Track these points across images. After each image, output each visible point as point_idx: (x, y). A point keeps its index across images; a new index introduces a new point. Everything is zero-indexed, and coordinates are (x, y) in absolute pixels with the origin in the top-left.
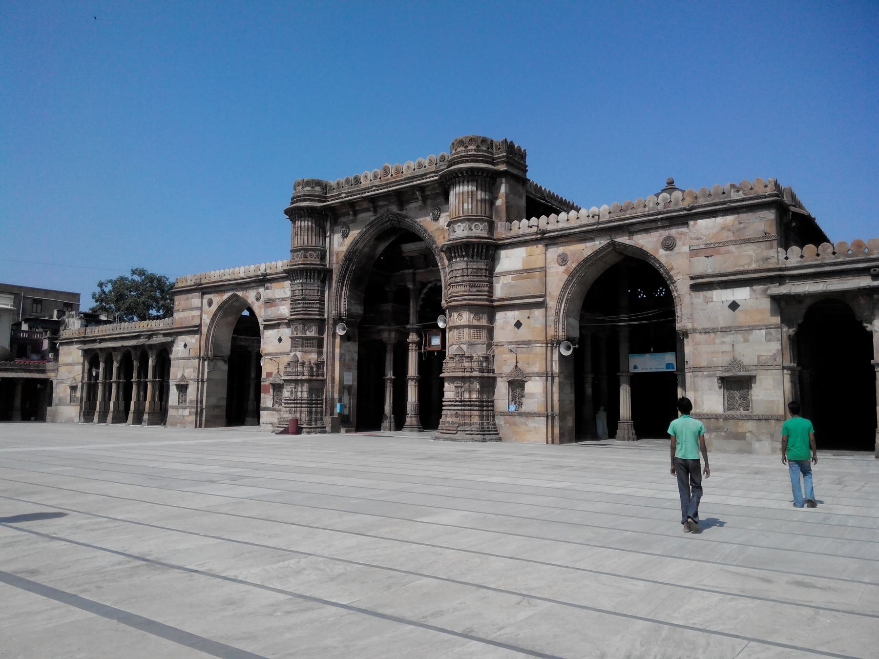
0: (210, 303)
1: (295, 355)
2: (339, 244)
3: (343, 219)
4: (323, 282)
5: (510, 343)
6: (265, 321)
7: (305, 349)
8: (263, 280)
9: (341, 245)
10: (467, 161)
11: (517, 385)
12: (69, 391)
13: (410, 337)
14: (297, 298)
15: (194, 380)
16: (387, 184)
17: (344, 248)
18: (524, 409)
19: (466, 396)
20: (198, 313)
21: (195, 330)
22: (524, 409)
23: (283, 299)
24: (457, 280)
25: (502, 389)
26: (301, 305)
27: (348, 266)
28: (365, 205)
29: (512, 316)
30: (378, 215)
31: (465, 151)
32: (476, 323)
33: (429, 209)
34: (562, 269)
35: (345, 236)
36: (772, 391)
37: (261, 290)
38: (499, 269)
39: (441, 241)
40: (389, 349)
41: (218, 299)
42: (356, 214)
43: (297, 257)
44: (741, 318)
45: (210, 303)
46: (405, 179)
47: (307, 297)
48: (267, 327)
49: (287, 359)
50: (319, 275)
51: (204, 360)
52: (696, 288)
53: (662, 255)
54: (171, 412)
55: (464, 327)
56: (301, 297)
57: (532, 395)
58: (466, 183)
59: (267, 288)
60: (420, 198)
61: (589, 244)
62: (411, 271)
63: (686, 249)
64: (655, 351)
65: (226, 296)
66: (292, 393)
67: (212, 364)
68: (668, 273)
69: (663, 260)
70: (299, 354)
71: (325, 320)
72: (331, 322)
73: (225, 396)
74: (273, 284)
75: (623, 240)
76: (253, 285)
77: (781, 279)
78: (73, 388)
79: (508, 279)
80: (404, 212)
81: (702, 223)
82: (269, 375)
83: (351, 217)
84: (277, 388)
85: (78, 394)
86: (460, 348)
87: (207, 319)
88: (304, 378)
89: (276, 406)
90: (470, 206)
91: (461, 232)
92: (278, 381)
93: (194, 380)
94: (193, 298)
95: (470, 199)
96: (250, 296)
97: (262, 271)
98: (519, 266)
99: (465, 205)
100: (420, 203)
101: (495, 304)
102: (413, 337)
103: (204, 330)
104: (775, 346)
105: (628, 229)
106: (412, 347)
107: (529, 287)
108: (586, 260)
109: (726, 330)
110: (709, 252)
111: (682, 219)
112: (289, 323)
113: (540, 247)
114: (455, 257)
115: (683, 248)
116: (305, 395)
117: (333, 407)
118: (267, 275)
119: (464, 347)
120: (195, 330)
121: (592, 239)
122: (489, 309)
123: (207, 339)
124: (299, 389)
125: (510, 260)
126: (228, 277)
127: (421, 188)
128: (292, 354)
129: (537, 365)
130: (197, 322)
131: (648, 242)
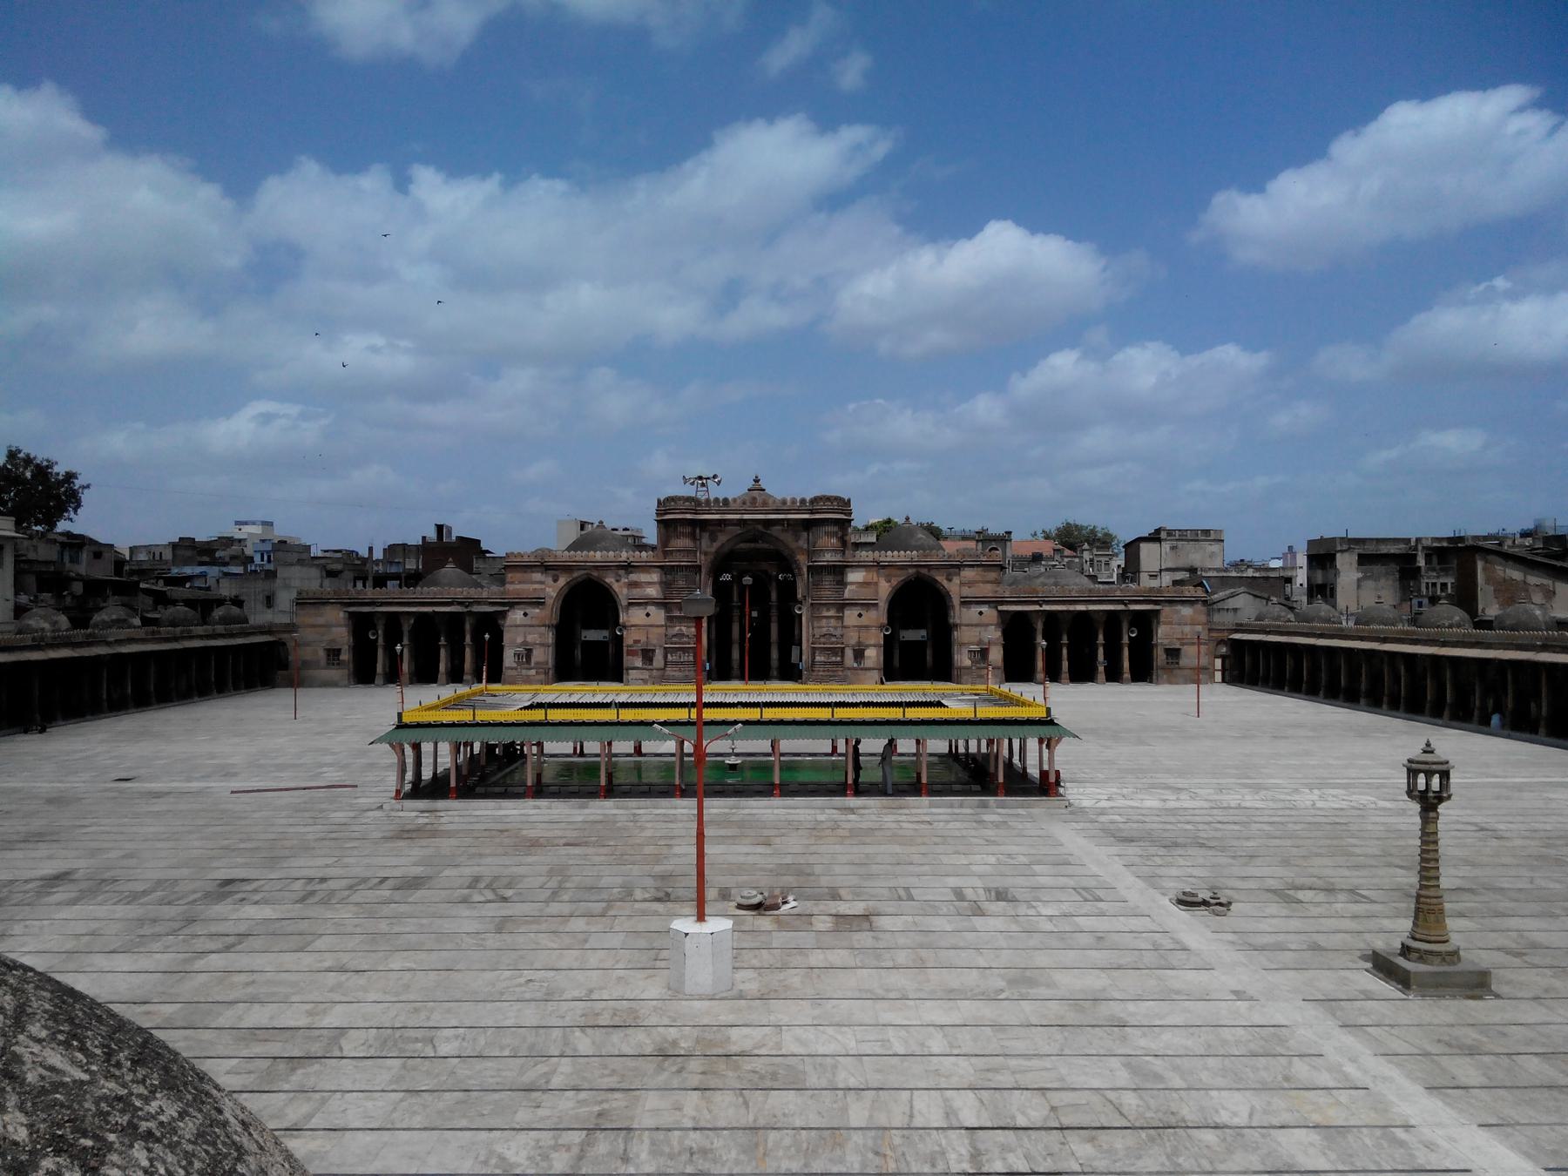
8: (628, 567)
11: (859, 654)
12: (322, 654)
15: (542, 645)
21: (538, 602)
25: (849, 653)
36: (996, 655)
37: (622, 572)
44: (984, 619)
45: (555, 581)
48: (630, 604)
52: (963, 603)
53: (945, 583)
54: (507, 673)
65: (576, 574)
77: (1002, 603)
78: (333, 654)
82: (637, 642)
84: (648, 655)
85: (345, 656)
91: (829, 558)
93: (542, 645)
103: (549, 602)
104: (999, 634)
107: (866, 593)
109: (976, 625)
111: (960, 567)
115: (956, 580)
120: (538, 602)
125: (854, 577)
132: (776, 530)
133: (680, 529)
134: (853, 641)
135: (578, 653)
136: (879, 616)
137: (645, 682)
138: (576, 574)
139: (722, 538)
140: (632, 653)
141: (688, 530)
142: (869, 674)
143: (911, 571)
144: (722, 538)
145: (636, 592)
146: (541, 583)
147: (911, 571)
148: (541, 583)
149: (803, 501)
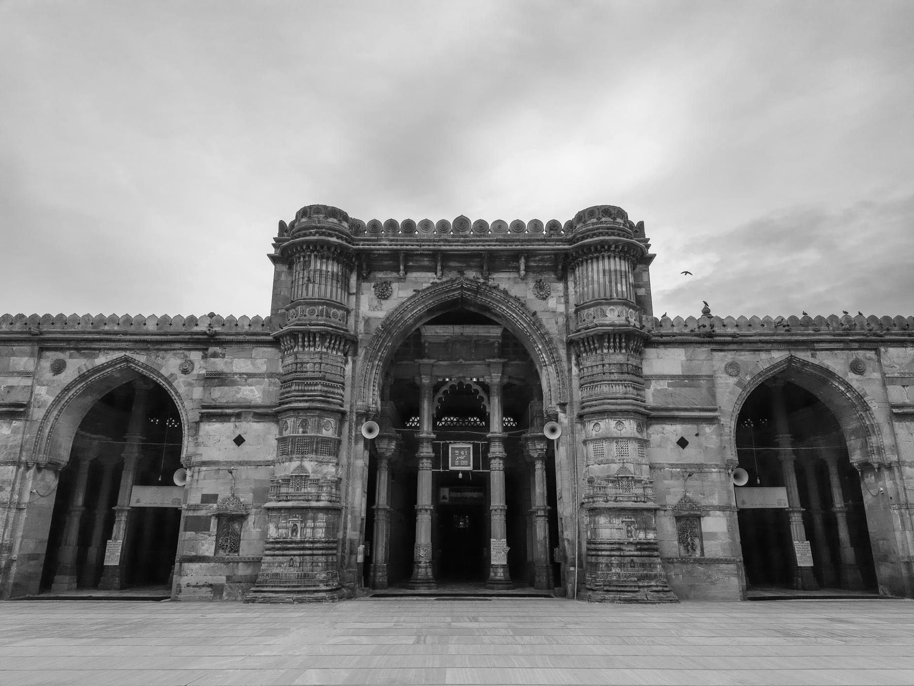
0: (58, 368)
1: (301, 467)
2: (372, 308)
3: (380, 275)
4: (346, 355)
5: (673, 466)
6: (204, 407)
7: (321, 458)
9: (373, 308)
10: (613, 234)
11: (689, 520)
13: (425, 450)
14: (309, 374)
16: (464, 242)
17: (381, 314)
18: (698, 554)
19: (642, 535)
20: (28, 382)
22: (698, 554)
23: (250, 375)
24: (612, 377)
26: (319, 387)
27: (384, 341)
28: (426, 262)
29: (674, 431)
30: (444, 279)
31: (614, 223)
32: (640, 437)
33: (532, 285)
34: (732, 380)
35: (383, 294)
37: (195, 356)
38: (646, 371)
39: (553, 327)
40: (384, 464)
41: (76, 365)
42: (408, 269)
43: (312, 312)
46: (497, 241)
47: (328, 376)
48: (207, 417)
49: (262, 474)
50: (344, 346)
51: (28, 468)
53: (852, 378)
55: (629, 439)
56: (316, 375)
57: (713, 535)
58: (617, 259)
59: (215, 355)
60: (522, 267)
61: (764, 356)
62: (432, 361)
63: (877, 375)
64: (761, 485)
66: (294, 530)
67: (39, 476)
68: (860, 397)
69: (855, 385)
70: (309, 465)
71: (343, 413)
72: (354, 418)
73: (46, 536)
74: (229, 349)
75: (804, 355)
76: (178, 346)
79: (663, 385)
80: (491, 283)
81: (894, 352)
82: (208, 499)
83: (402, 273)
84: (230, 522)
86: (623, 469)
87: (45, 395)
88: (321, 504)
89: (221, 553)
90: (624, 289)
92: (232, 508)
94: (13, 354)
95: (624, 280)
96: (169, 365)
97: (203, 327)
98: (678, 371)
99: (619, 285)
100: (523, 273)
101: (654, 414)
102: (426, 450)
103: (38, 414)
105: (808, 345)
106: (426, 464)
108: (759, 375)
110: (905, 382)
112: (270, 414)
113: (702, 352)
114: (609, 348)
116: (320, 534)
117: (353, 552)
118: (216, 333)
119: (631, 467)
121: (768, 351)
122: (648, 417)
123: (41, 430)
124: (310, 523)
125: (664, 362)
126: (116, 328)
127: (529, 255)
128: (295, 464)
129: (716, 496)
130: (22, 398)
131: (835, 362)
132: (503, 280)
133: (317, 264)
134: (672, 500)
135: (120, 529)
136: (716, 443)
137: (217, 591)
138: (101, 360)
139: (401, 293)
140: (200, 525)
141: (333, 268)
142: (716, 573)
143: (779, 356)
144: (401, 293)
145: (219, 394)
146: (26, 374)
147: (779, 356)
148: (26, 374)
149: (554, 226)
